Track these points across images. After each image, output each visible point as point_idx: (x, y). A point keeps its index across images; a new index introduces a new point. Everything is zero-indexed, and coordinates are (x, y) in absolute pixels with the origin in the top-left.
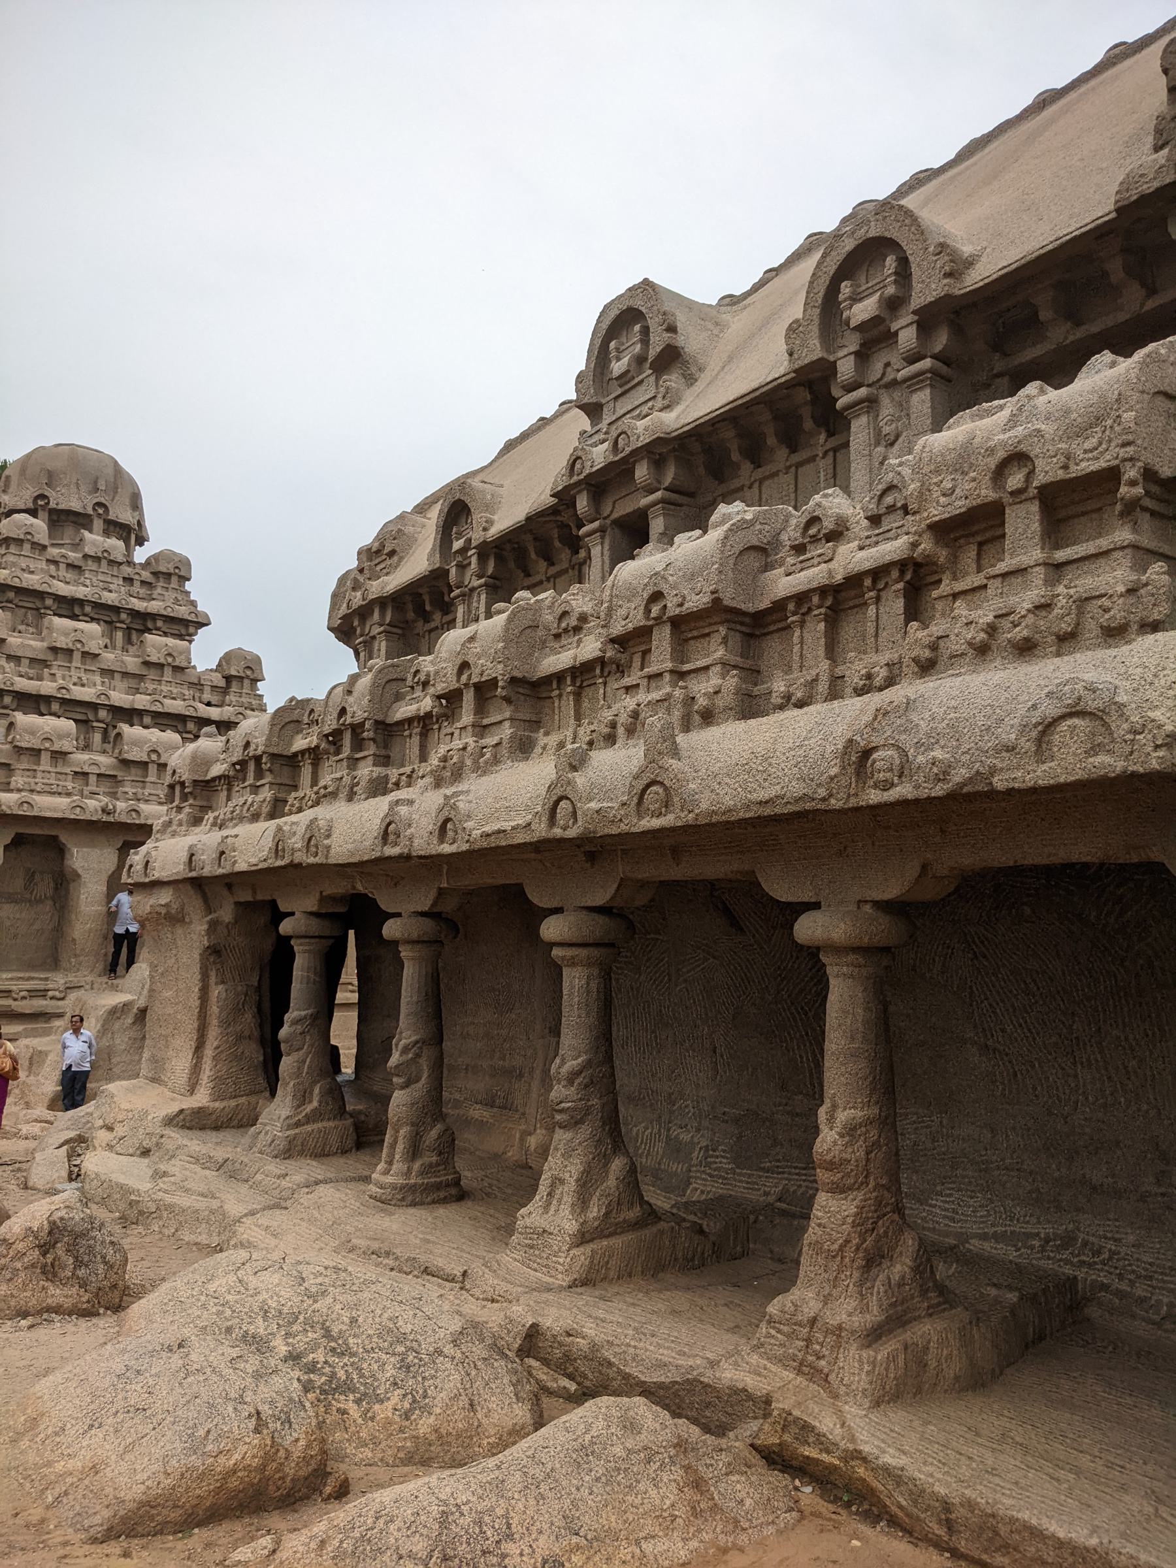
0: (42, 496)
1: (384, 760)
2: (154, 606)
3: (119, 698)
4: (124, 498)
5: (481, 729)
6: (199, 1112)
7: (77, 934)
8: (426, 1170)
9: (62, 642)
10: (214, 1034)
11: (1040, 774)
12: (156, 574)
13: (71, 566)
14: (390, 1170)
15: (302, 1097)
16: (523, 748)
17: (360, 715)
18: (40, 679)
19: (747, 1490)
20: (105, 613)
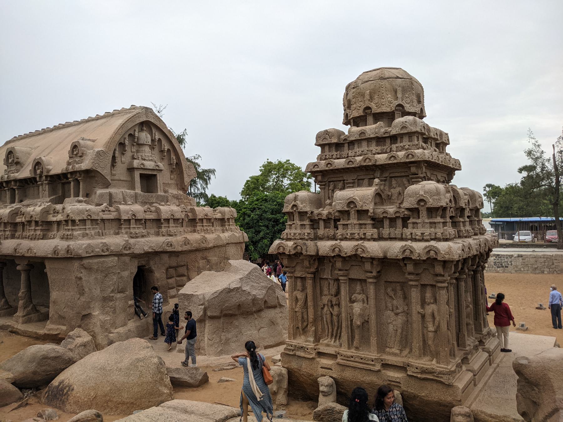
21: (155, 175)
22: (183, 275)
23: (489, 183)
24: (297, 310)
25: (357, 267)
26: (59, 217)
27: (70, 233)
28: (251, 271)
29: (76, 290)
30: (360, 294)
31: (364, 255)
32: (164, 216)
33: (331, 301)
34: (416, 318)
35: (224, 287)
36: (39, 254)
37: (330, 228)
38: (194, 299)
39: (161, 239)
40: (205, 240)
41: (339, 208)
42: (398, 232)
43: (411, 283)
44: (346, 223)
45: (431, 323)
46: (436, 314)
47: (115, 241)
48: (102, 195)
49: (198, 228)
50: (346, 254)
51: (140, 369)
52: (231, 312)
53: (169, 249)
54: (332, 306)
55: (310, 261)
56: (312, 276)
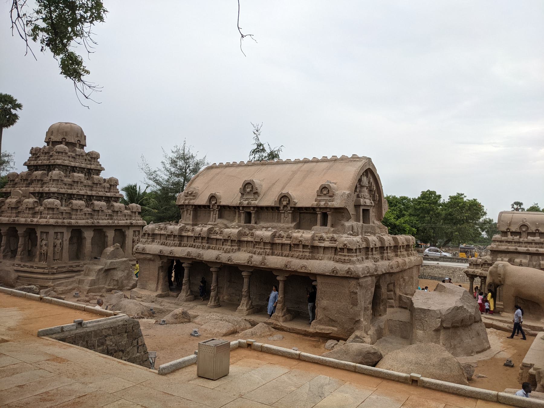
0: (64, 138)
1: (208, 243)
2: (93, 167)
3: (89, 193)
4: (83, 137)
5: (232, 246)
6: (161, 295)
7: (85, 252)
8: (217, 303)
9: (76, 180)
10: (161, 281)
11: (301, 271)
12: (91, 158)
13: (73, 157)
14: (211, 303)
15: (187, 292)
16: (239, 250)
17: (204, 236)
18: (71, 189)
19: (273, 329)
20: (81, 170)
21: (368, 210)
22: (391, 291)
23: (516, 201)
26: (327, 244)
27: (347, 258)
29: (348, 301)
32: (387, 244)
35: (454, 305)
36: (314, 271)
38: (431, 313)
39: (386, 263)
40: (405, 263)
47: (369, 264)
48: (349, 227)
49: (399, 253)
51: (450, 365)
52: (457, 325)
53: (391, 271)
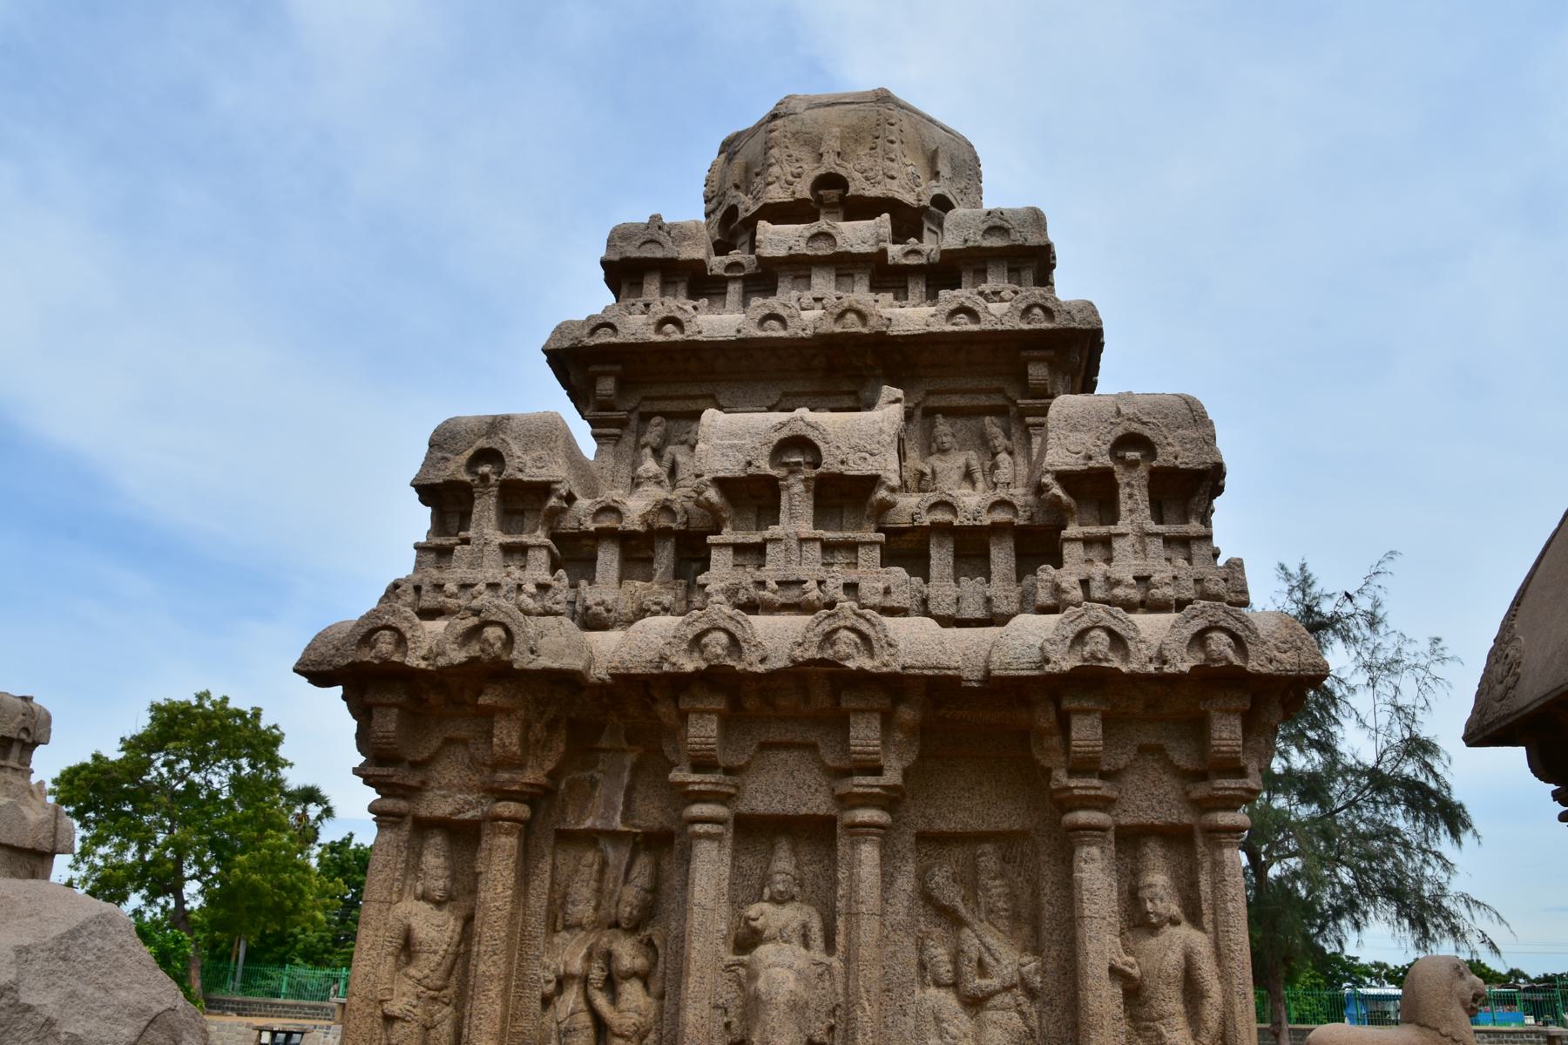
24: (396, 1007)
25: (791, 758)
28: (83, 927)
30: (779, 900)
31: (868, 664)
33: (609, 956)
34: (1103, 999)
37: (649, 578)
41: (730, 467)
42: (1001, 585)
43: (1083, 817)
44: (756, 538)
45: (1180, 1021)
46: (1207, 969)
50: (763, 660)
54: (611, 985)
55: (527, 727)
56: (523, 810)
